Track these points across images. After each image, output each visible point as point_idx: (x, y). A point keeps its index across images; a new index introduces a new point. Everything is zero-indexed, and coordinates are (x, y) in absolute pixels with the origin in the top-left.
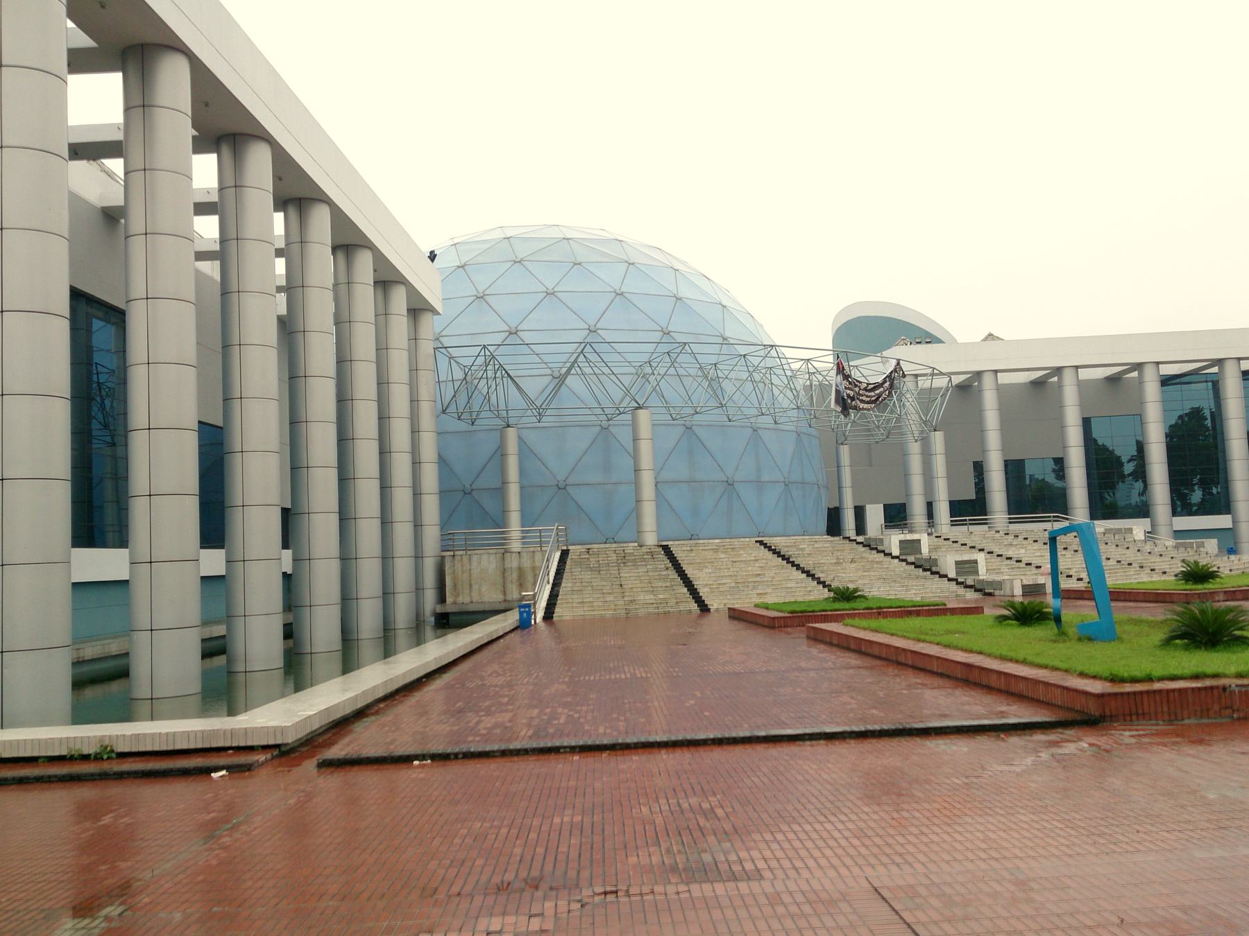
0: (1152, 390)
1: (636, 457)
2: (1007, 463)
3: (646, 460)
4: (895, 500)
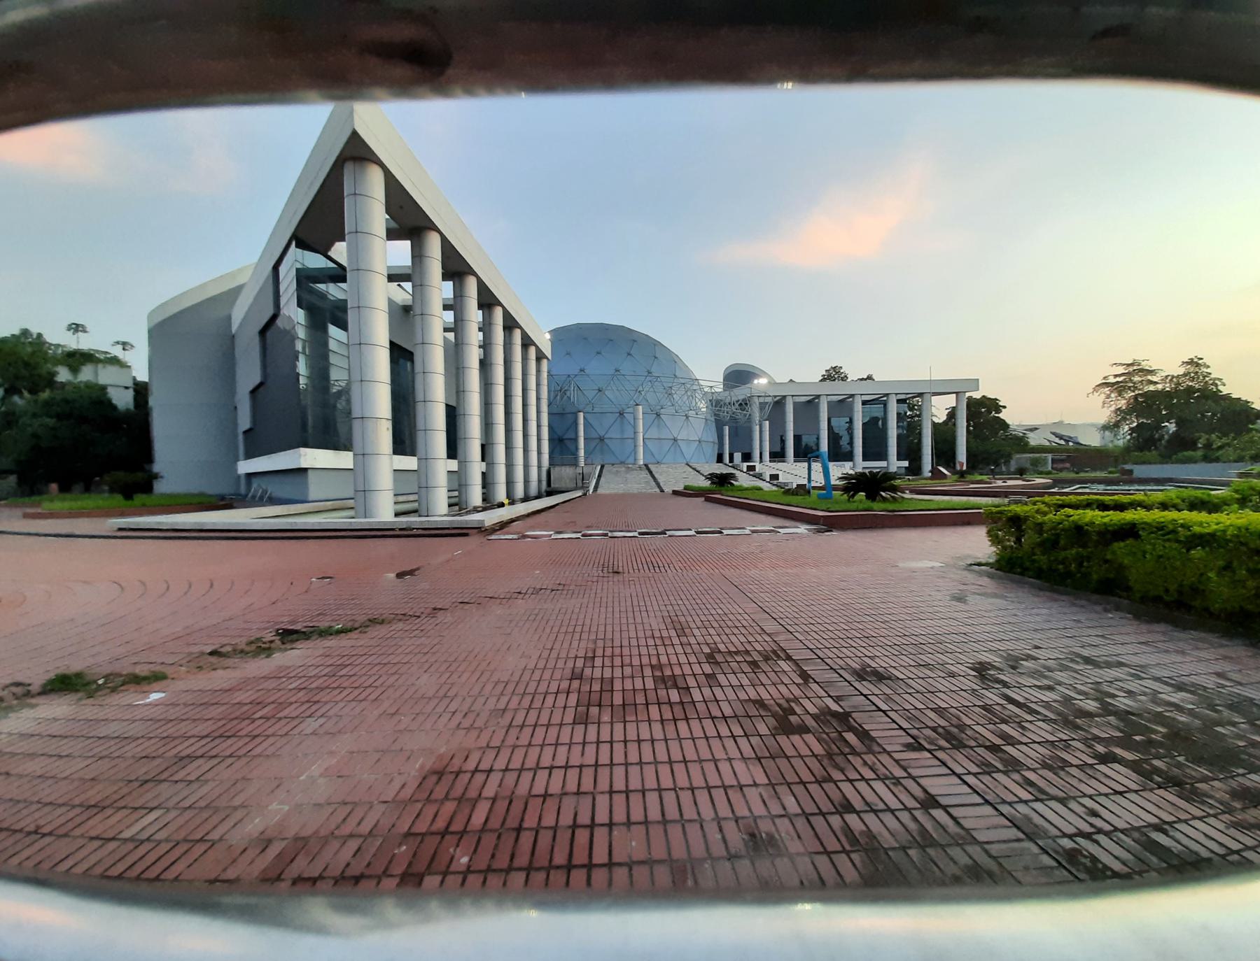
0: (858, 407)
1: (635, 427)
2: (795, 436)
3: (641, 429)
4: (746, 451)
